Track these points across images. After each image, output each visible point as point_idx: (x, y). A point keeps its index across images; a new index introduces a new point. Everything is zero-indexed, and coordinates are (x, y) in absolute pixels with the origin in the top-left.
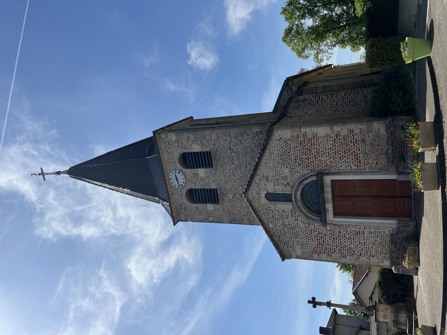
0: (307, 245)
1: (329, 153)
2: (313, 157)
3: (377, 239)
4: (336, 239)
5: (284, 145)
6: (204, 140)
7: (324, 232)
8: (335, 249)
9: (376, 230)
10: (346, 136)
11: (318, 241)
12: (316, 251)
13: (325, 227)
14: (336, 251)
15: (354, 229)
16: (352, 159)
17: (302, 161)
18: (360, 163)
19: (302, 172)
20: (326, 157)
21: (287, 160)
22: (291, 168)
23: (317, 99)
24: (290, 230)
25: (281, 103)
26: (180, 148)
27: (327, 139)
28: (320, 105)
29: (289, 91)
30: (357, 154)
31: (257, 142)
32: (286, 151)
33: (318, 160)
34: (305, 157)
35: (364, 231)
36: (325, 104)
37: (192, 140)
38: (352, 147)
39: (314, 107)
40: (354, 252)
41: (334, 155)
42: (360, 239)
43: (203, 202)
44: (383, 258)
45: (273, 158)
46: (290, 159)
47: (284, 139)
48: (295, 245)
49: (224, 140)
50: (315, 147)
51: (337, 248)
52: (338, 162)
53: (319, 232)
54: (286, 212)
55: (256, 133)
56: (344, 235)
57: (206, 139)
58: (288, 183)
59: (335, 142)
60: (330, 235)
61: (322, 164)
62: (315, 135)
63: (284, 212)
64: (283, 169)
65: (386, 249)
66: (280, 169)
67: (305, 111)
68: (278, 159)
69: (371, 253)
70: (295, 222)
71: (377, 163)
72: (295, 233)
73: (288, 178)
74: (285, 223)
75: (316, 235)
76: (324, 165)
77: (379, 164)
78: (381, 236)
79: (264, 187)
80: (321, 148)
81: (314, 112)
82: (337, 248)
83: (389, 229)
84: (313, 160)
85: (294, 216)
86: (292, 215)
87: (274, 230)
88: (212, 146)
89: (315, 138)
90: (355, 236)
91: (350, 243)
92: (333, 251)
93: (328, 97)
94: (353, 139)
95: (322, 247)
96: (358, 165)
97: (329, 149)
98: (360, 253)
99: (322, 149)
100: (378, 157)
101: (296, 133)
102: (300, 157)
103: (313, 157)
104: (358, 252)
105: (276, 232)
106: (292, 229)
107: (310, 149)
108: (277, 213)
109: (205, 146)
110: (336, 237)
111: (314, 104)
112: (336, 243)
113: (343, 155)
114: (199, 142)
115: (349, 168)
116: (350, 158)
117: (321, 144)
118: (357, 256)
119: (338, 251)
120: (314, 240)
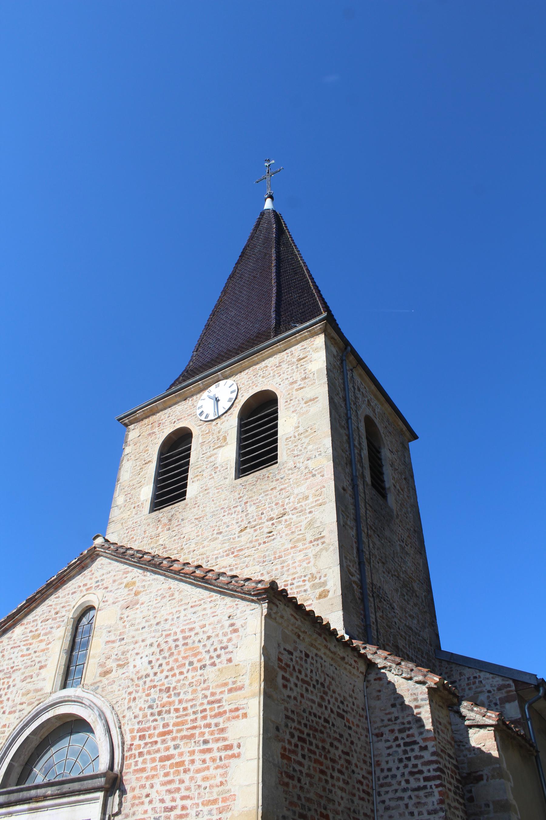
1: (172, 809)
2: (167, 749)
6: (307, 440)
17: (160, 713)
19: (129, 715)
20: (162, 801)
21: (171, 660)
22: (147, 676)
23: (425, 769)
25: (468, 673)
28: (407, 781)
29: (502, 694)
31: (298, 587)
32: (195, 655)
36: (411, 803)
37: (307, 411)
39: (400, 760)
43: (158, 474)
47: (234, 641)
50: (197, 757)
55: (323, 580)
61: (143, 787)
62: (236, 751)
63: (41, 668)
64: (149, 651)
66: (148, 642)
67: (386, 730)
68: (178, 631)
76: (137, 792)
79: (111, 601)
80: (192, 779)
81: (384, 766)
84: (158, 751)
88: (291, 464)
89: (223, 754)
93: (435, 812)
97: (184, 808)
99: (187, 783)
101: (247, 683)
108: (43, 646)
109: (291, 446)
111: (409, 759)
114: (301, 430)
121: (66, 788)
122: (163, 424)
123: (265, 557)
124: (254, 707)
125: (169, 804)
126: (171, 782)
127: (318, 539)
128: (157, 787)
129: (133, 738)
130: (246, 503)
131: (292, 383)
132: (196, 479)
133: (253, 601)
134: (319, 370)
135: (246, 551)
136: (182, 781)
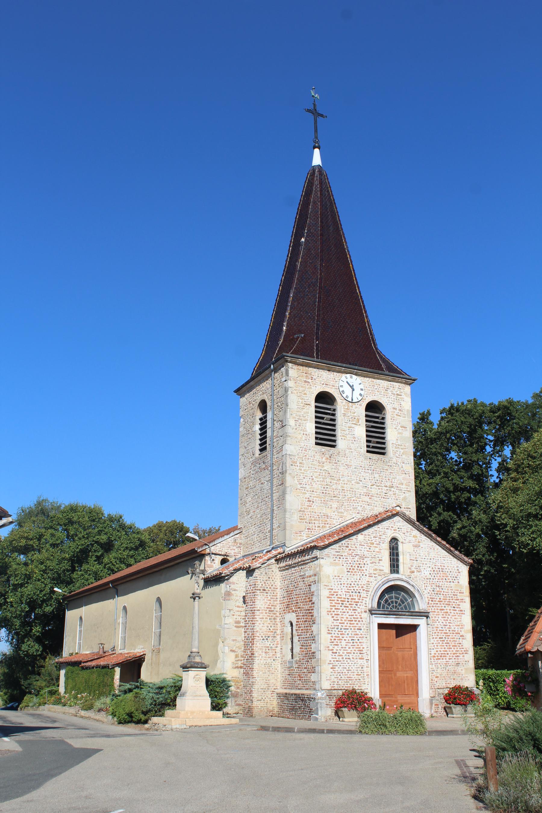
0: (340, 583)
1: (446, 625)
2: (442, 607)
3: (355, 674)
4: (350, 624)
5: (453, 575)
7: (358, 609)
8: (338, 620)
9: (365, 674)
10: (462, 646)
11: (347, 600)
12: (333, 595)
13: (365, 612)
14: (335, 622)
15: (365, 647)
16: (440, 651)
17: (437, 594)
18: (437, 659)
19: (426, 591)
22: (430, 579)
24: (356, 564)
26: (392, 410)
27: (459, 626)
30: (446, 656)
32: (447, 577)
33: (438, 612)
34: (442, 598)
35: (363, 659)
38: (452, 651)
40: (336, 645)
41: (445, 631)
42: (354, 653)
44: (332, 680)
45: (439, 559)
46: (439, 579)
48: (337, 567)
49: (403, 481)
50: (452, 611)
51: (340, 623)
52: (437, 635)
53: (358, 602)
54: (379, 563)
56: (357, 634)
57: (403, 453)
58: (413, 572)
59: (456, 633)
60: (355, 617)
61: (435, 617)
62: (463, 612)
63: (380, 560)
65: (344, 684)
66: (428, 565)
68: (439, 565)
69: (337, 666)
70: (368, 572)
71: (437, 677)
72: (353, 569)
73: (418, 574)
74: (366, 559)
75: (354, 597)
76: (434, 618)
77: (436, 679)
78: (360, 680)
82: (340, 623)
83: (369, 688)
85: (375, 572)
86: (376, 570)
87: (355, 540)
90: (357, 648)
91: (347, 641)
92: (335, 618)
94: (460, 654)
95: (339, 604)
96: (434, 657)
98: (336, 653)
100: (443, 678)
102: (441, 592)
103: (442, 607)
104: (337, 650)
105: (353, 543)
106: (358, 567)
107: (449, 604)
108: (377, 550)
110: (353, 624)
112: (346, 622)
113: (444, 641)
114: (399, 443)
115: (431, 646)
116: (442, 648)
117: (455, 618)
118: (331, 648)
119: (335, 624)
120: (347, 594)
121: (414, 614)
122: (315, 379)
123: (384, 505)
124: (468, 600)
125: (445, 624)
126: (445, 617)
127: (408, 508)
128: (440, 618)
129: (429, 600)
130: (373, 470)
131: (394, 408)
132: (343, 438)
133: (466, 565)
134: (408, 410)
135: (375, 498)
136: (448, 618)
